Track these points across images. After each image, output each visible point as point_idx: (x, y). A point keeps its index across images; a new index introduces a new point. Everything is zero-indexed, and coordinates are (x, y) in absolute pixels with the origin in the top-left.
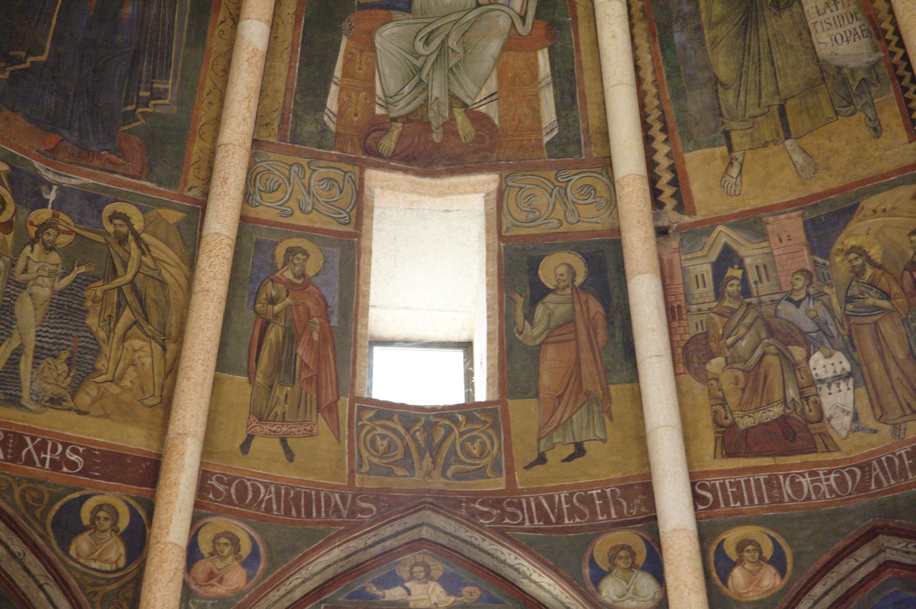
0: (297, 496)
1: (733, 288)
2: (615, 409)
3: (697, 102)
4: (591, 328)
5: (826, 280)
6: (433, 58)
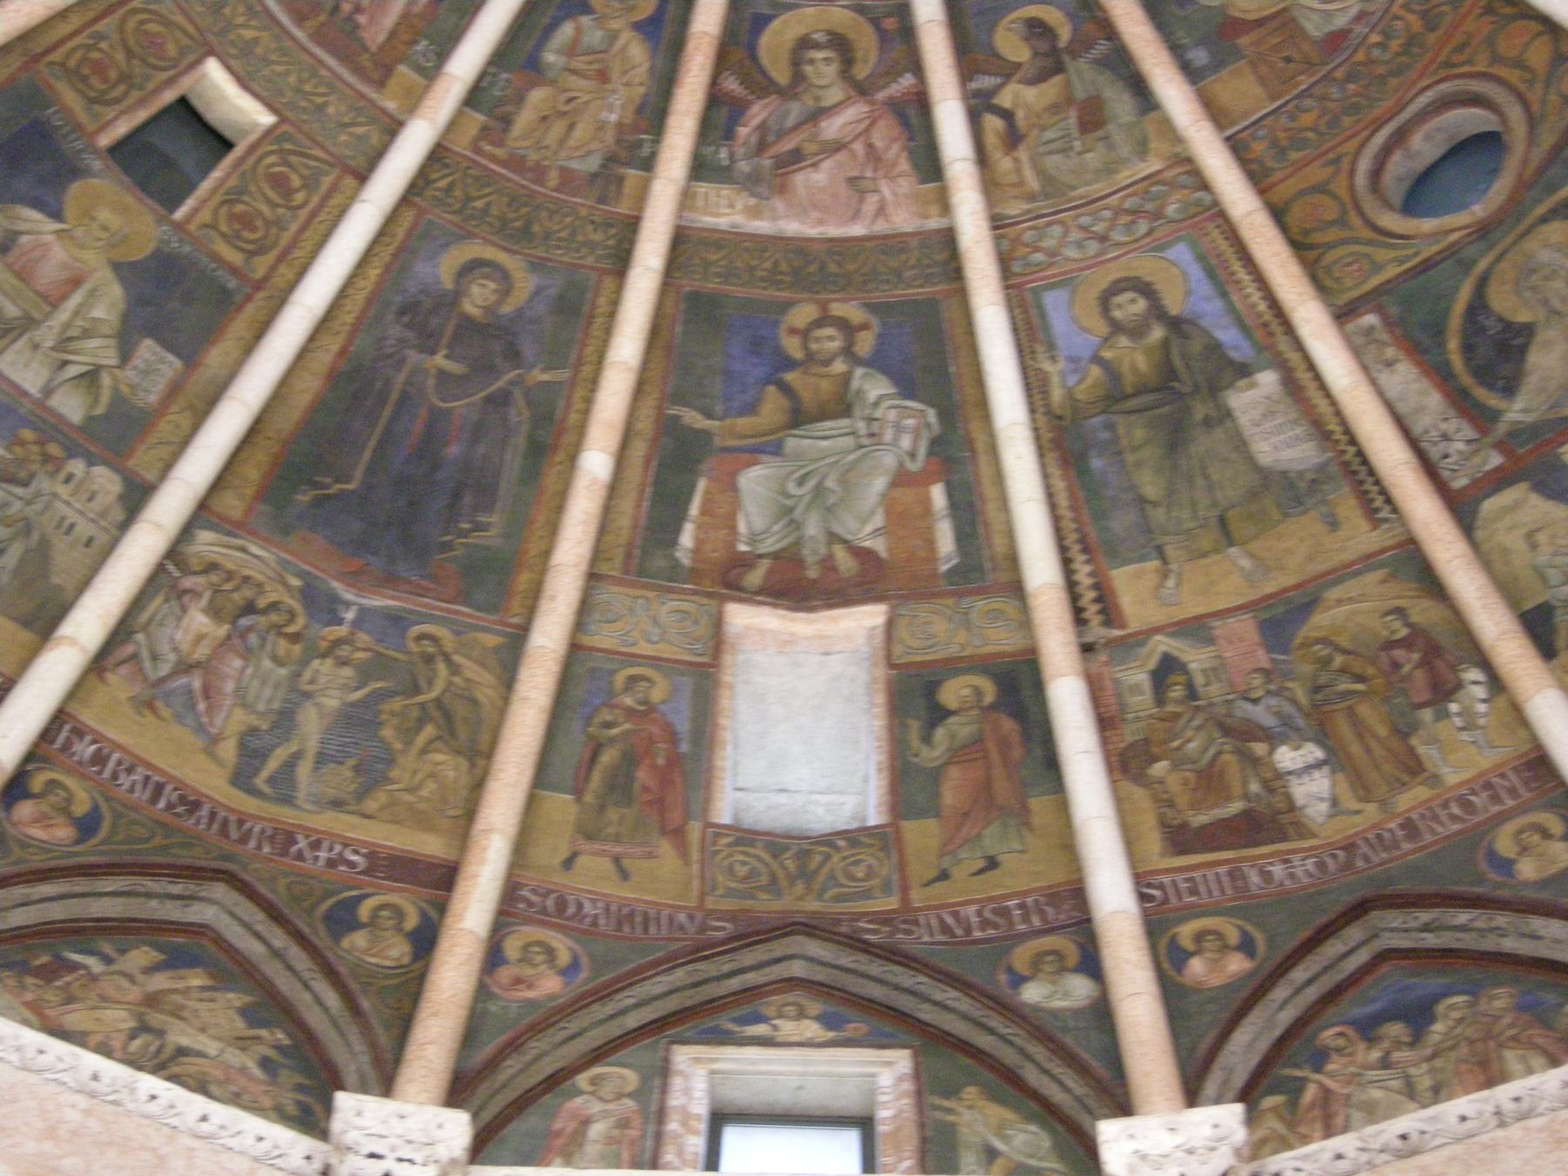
0: (631, 915)
1: (1177, 692)
2: (1036, 820)
3: (1121, 522)
4: (1004, 744)
5: (1288, 675)
6: (806, 499)
